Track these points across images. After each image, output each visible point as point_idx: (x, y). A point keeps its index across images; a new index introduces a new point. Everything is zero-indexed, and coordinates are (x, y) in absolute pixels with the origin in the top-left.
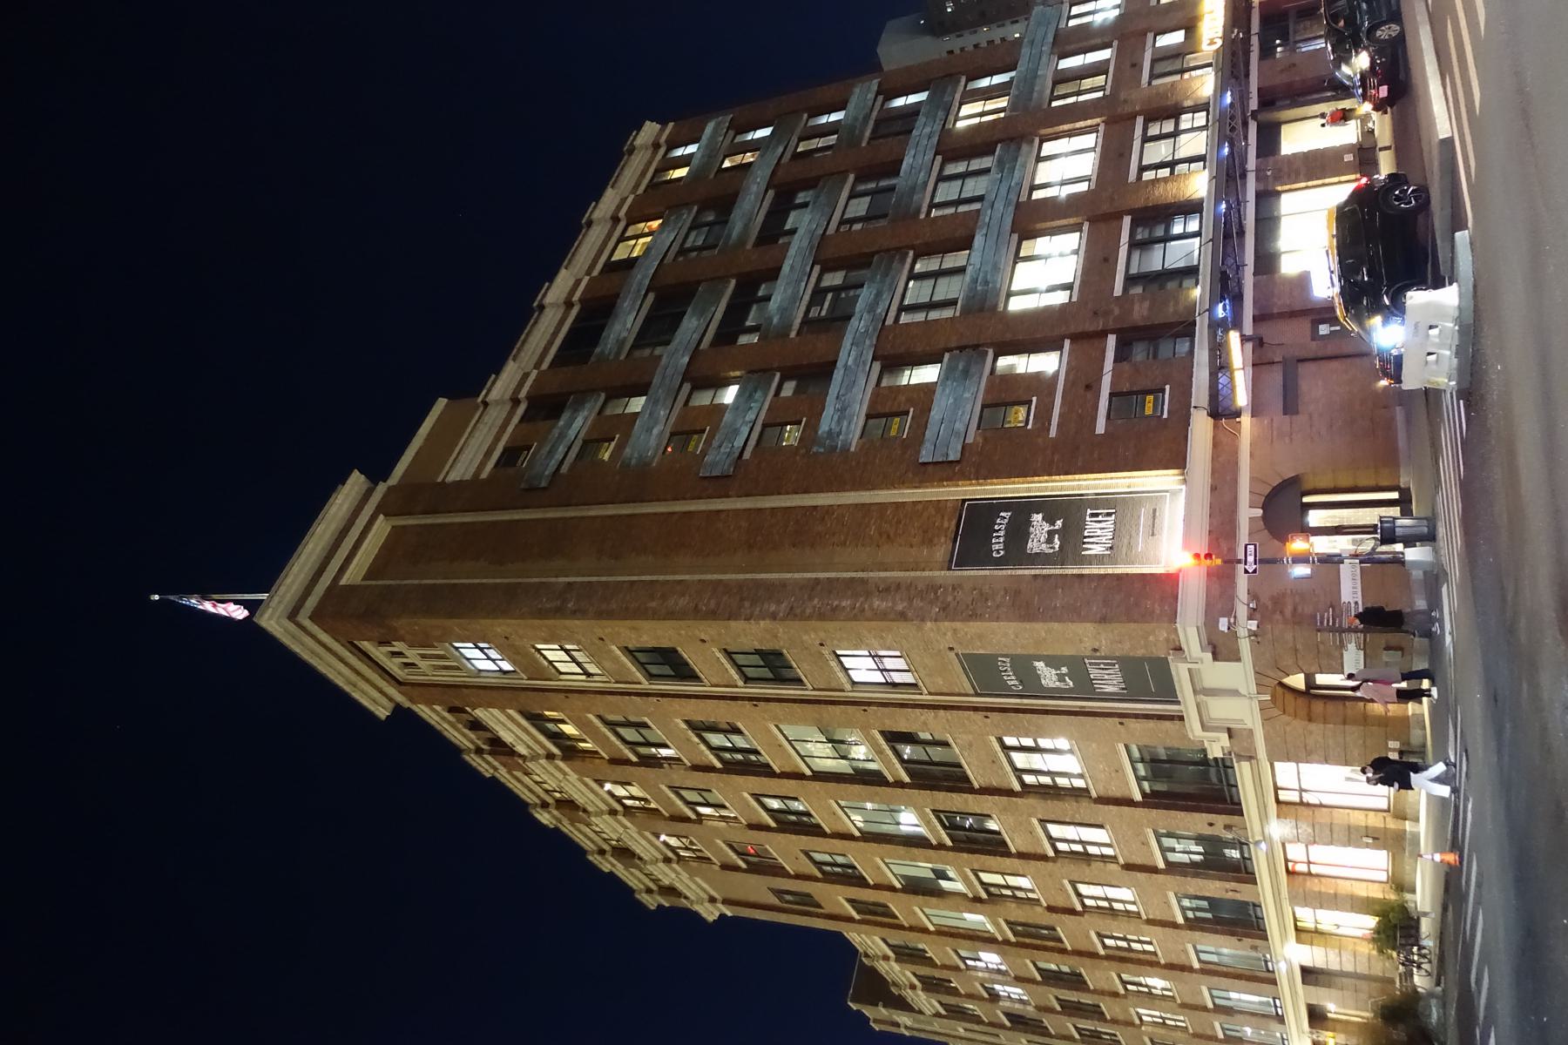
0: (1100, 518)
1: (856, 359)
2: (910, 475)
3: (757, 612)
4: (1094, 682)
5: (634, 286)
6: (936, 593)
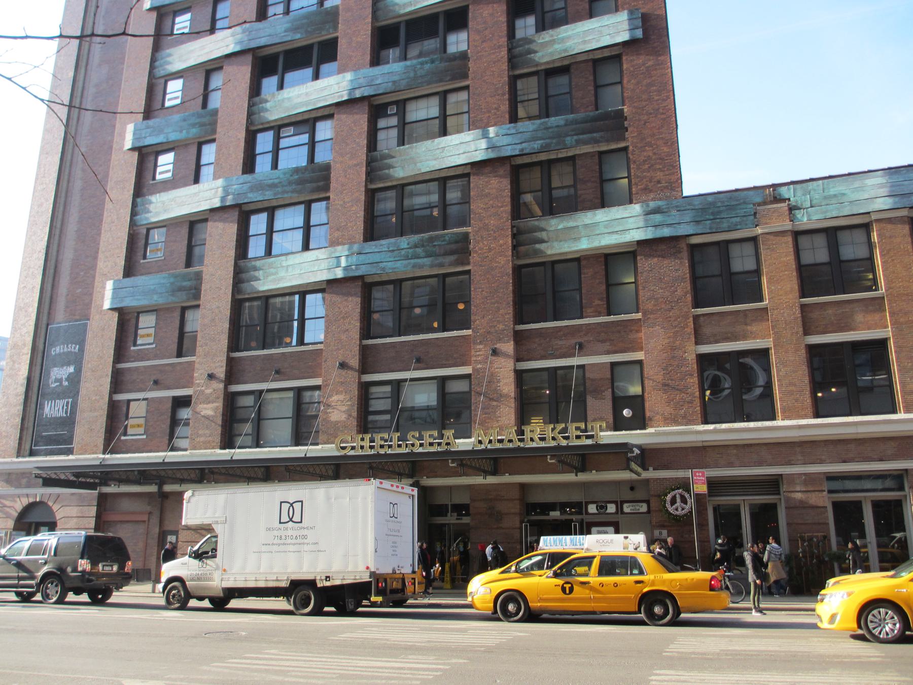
0: (65, 407)
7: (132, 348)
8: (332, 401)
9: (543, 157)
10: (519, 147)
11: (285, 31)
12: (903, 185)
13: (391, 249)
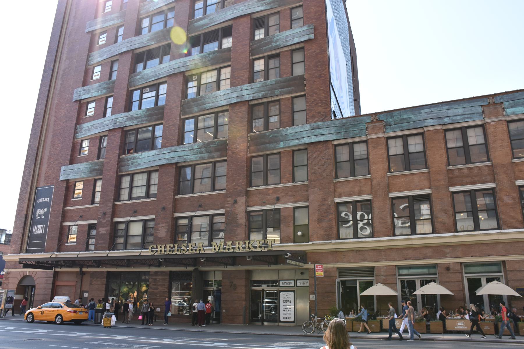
7: (72, 200)
8: (160, 227)
9: (265, 100)
10: (252, 96)
11: (147, 41)
12: (439, 113)
13: (189, 149)
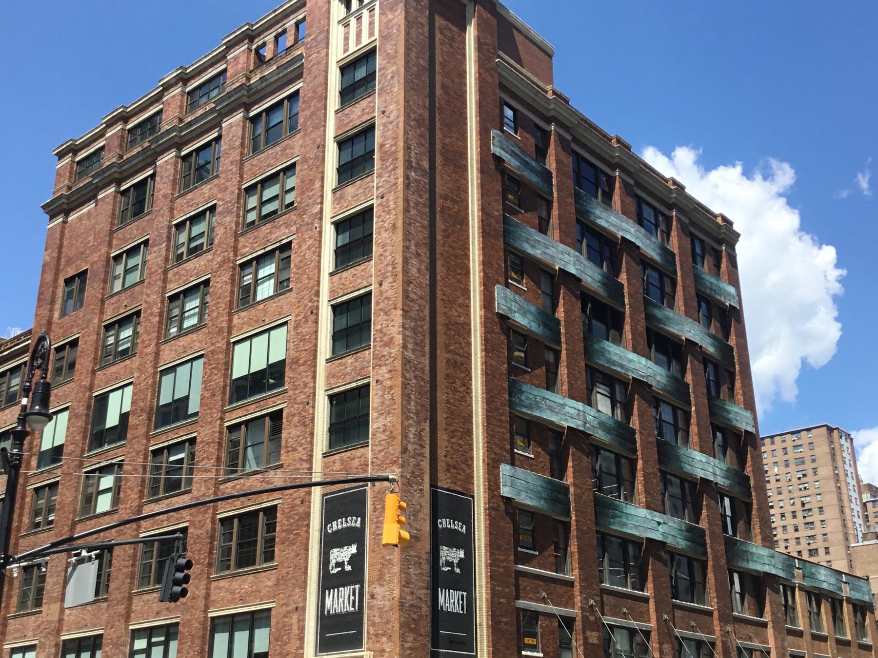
0: (461, 602)
1: (569, 413)
2: (493, 456)
3: (407, 333)
4: (336, 590)
5: (626, 226)
6: (419, 476)
